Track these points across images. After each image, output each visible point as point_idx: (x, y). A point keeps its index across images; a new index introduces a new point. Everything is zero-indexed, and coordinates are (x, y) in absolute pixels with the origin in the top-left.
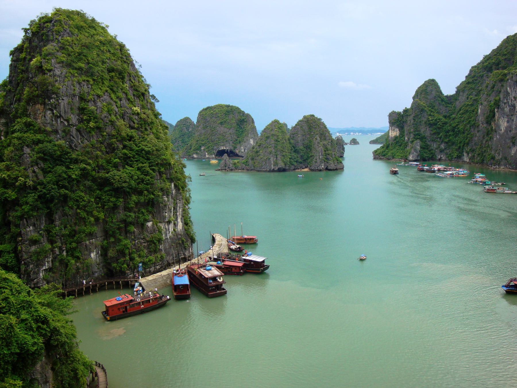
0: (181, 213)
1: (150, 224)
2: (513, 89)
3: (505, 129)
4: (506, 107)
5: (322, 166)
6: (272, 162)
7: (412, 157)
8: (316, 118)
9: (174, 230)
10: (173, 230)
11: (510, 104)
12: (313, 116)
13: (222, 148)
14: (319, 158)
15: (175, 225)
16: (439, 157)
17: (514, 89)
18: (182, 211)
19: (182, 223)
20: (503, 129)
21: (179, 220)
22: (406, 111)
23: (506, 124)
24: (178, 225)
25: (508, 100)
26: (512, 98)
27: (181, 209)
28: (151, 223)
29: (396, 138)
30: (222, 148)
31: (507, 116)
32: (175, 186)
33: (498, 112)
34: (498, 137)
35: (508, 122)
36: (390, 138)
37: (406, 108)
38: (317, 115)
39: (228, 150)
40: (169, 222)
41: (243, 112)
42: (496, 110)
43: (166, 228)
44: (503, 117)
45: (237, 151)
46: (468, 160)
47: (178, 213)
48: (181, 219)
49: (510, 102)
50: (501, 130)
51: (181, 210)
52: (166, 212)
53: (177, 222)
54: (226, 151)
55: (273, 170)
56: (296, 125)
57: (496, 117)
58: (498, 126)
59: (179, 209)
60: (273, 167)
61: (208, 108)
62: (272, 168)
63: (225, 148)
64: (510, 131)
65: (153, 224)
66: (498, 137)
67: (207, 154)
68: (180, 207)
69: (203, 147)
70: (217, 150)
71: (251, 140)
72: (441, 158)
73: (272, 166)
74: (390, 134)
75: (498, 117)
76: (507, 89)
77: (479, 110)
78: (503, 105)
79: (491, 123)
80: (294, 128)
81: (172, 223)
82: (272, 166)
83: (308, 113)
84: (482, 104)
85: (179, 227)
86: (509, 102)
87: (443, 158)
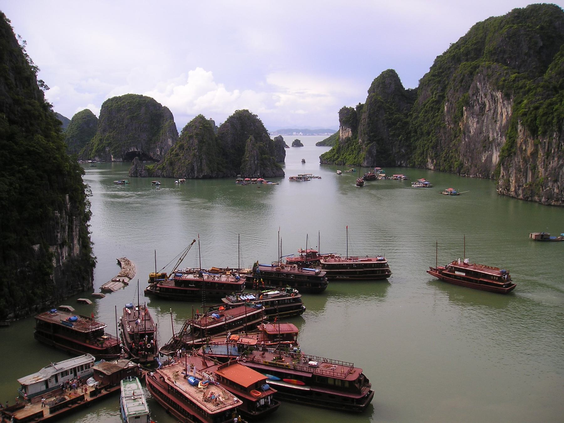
0: (78, 232)
1: (36, 247)
2: (483, 84)
3: (474, 131)
4: (476, 105)
7: (367, 163)
9: (69, 255)
10: (67, 255)
11: (480, 102)
12: (247, 111)
13: (133, 150)
15: (71, 249)
16: (399, 163)
17: (484, 84)
19: (79, 245)
20: (472, 132)
21: (76, 242)
22: (360, 107)
23: (475, 126)
24: (75, 249)
25: (478, 98)
26: (483, 95)
28: (38, 245)
29: (348, 139)
30: (132, 150)
31: (477, 115)
32: (71, 198)
33: (466, 110)
34: (467, 140)
35: (478, 122)
36: (341, 139)
37: (360, 103)
39: (139, 152)
40: (62, 246)
42: (464, 108)
43: (58, 252)
44: (473, 117)
45: (152, 154)
46: (432, 168)
48: (79, 240)
49: (480, 100)
50: (470, 132)
52: (58, 232)
53: (73, 244)
54: (137, 153)
56: (226, 122)
57: (465, 117)
58: (467, 127)
63: (136, 150)
64: (480, 133)
65: (41, 248)
66: (467, 140)
67: (112, 156)
68: (76, 225)
71: (169, 140)
72: (401, 164)
73: (196, 172)
75: (467, 116)
76: (477, 84)
77: (445, 108)
78: (473, 103)
79: (459, 124)
80: (223, 126)
84: (448, 101)
85: (75, 251)
86: (478, 99)
87: (404, 165)
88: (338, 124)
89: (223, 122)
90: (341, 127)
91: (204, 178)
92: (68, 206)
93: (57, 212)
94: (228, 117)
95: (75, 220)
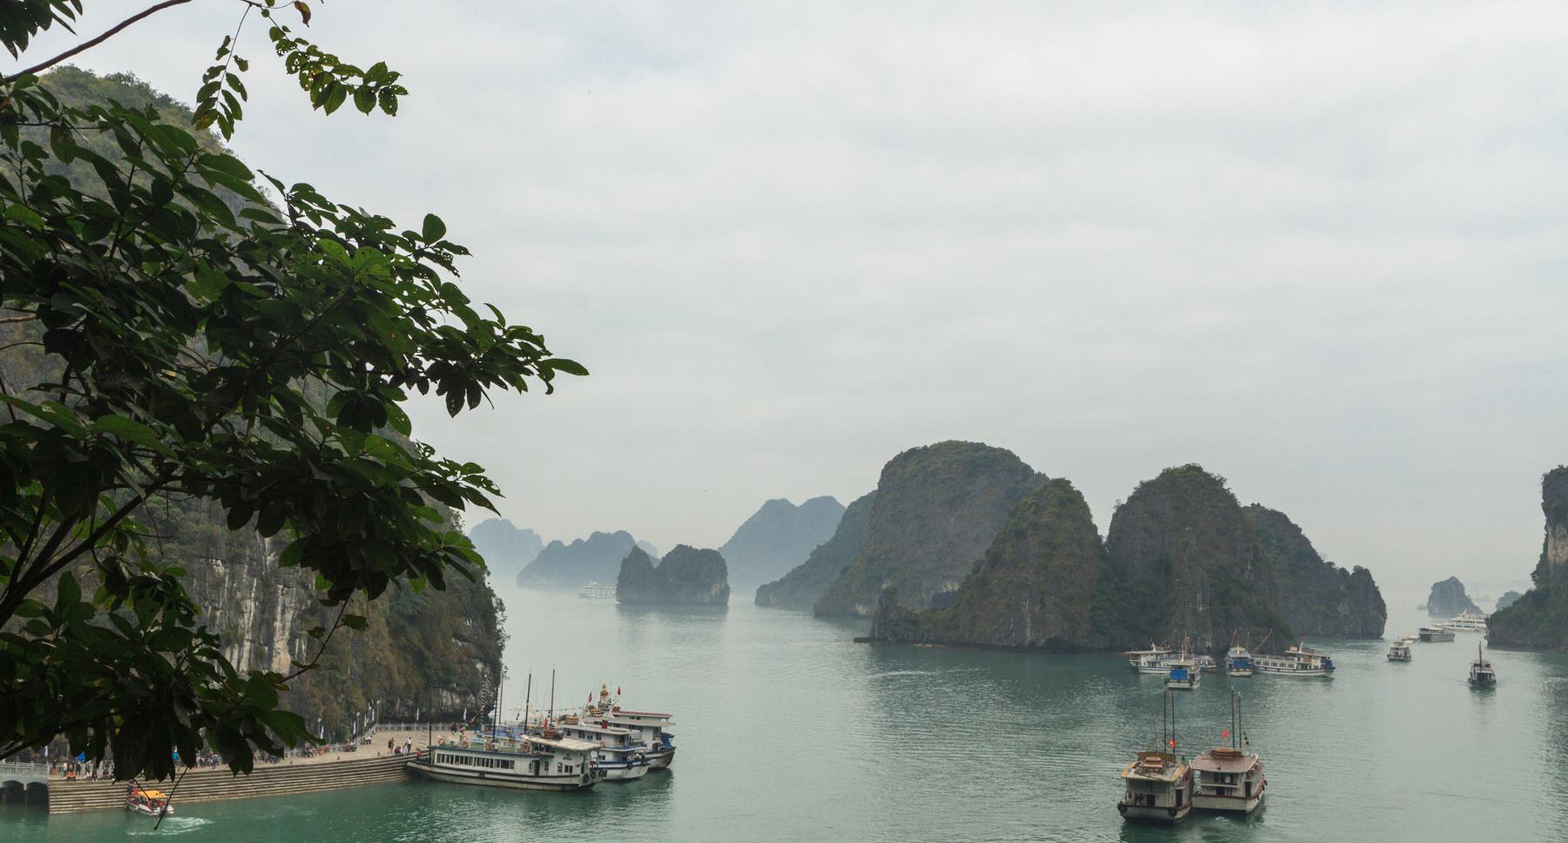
0: (288, 625)
5: (1203, 640)
6: (1028, 619)
8: (1207, 475)
14: (1195, 612)
15: (262, 654)
18: (293, 620)
21: (280, 644)
27: (292, 612)
38: (1211, 468)
41: (1027, 468)
47: (278, 624)
48: (291, 643)
51: (289, 616)
52: (215, 609)
53: (271, 648)
55: (1032, 644)
56: (1130, 499)
59: (283, 612)
60: (1029, 635)
61: (913, 452)
62: (1029, 640)
68: (284, 606)
69: (889, 581)
70: (933, 593)
73: (1028, 630)
74: (1551, 553)
81: (241, 645)
82: (1028, 630)
83: (1178, 462)
88: (1542, 519)
89: (1124, 501)
90: (1550, 529)
91: (1057, 648)
92: (269, 558)
93: (219, 562)
94: (1138, 485)
95: (283, 594)
